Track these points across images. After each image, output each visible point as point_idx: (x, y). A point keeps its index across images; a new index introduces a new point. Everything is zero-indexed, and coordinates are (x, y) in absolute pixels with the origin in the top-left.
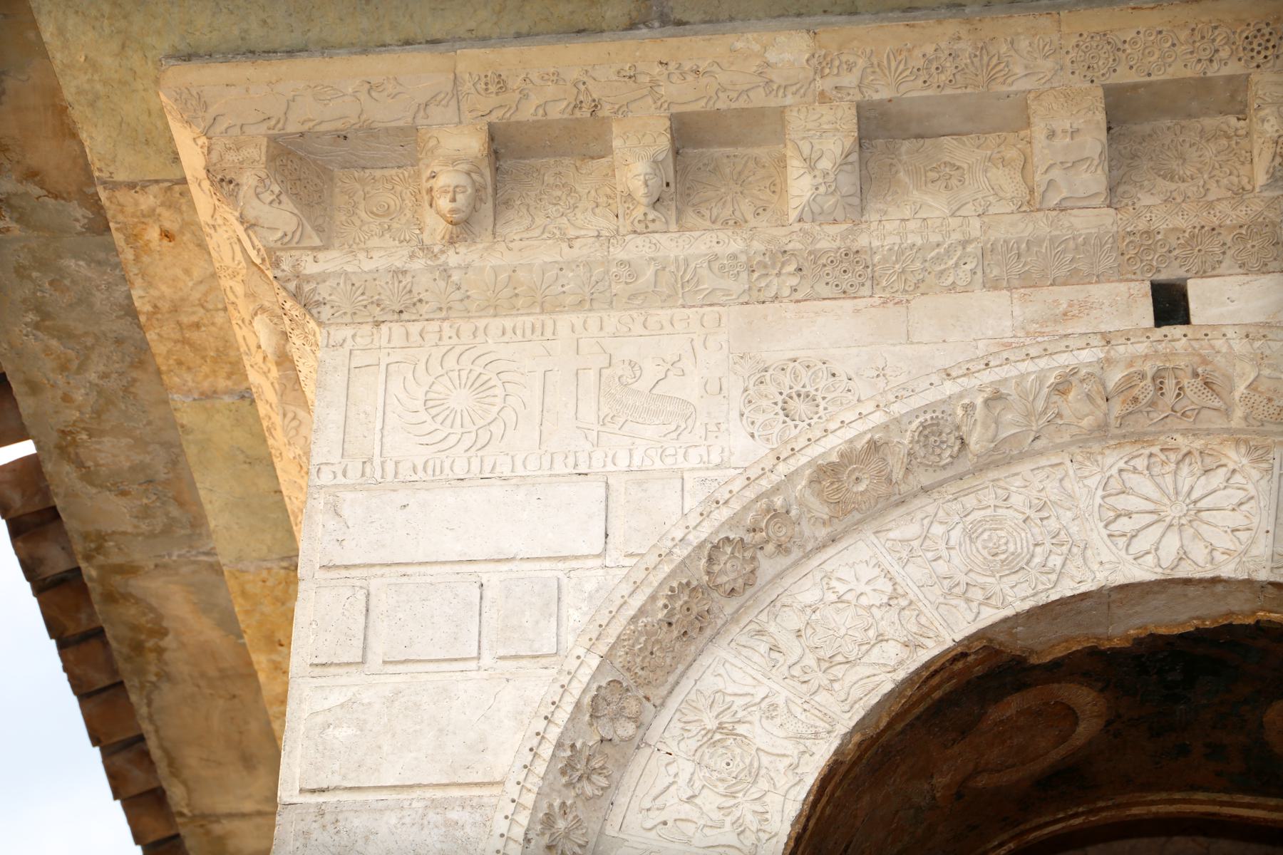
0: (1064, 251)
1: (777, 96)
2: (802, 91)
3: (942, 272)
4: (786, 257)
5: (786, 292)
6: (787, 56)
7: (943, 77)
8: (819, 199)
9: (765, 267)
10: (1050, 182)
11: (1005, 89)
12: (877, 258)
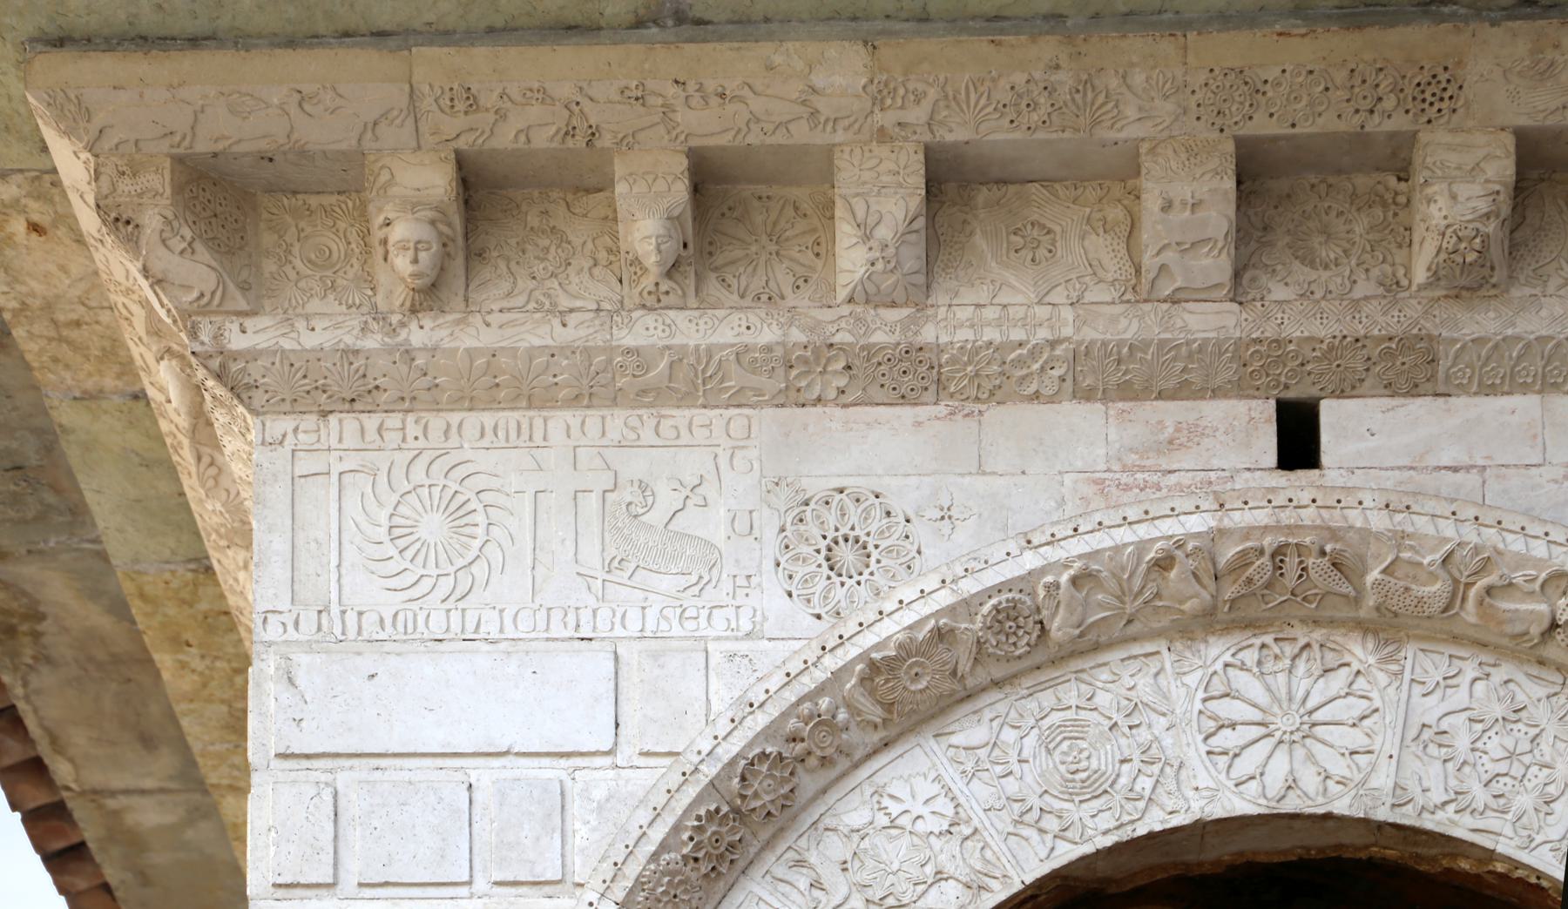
2: (856, 126)
7: (1035, 117)
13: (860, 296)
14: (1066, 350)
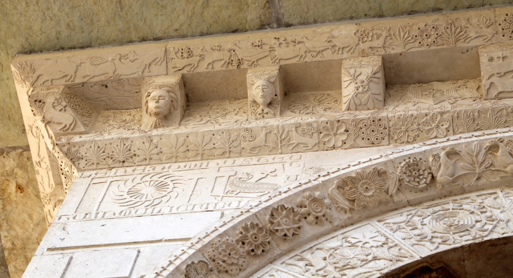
0: (501, 116)
1: (338, 53)
2: (352, 50)
3: (429, 131)
4: (340, 124)
5: (340, 144)
6: (344, 32)
7: (430, 40)
8: (359, 95)
9: (328, 130)
10: (491, 83)
11: (465, 45)
12: (391, 124)
13: (352, 106)
14: (448, 116)
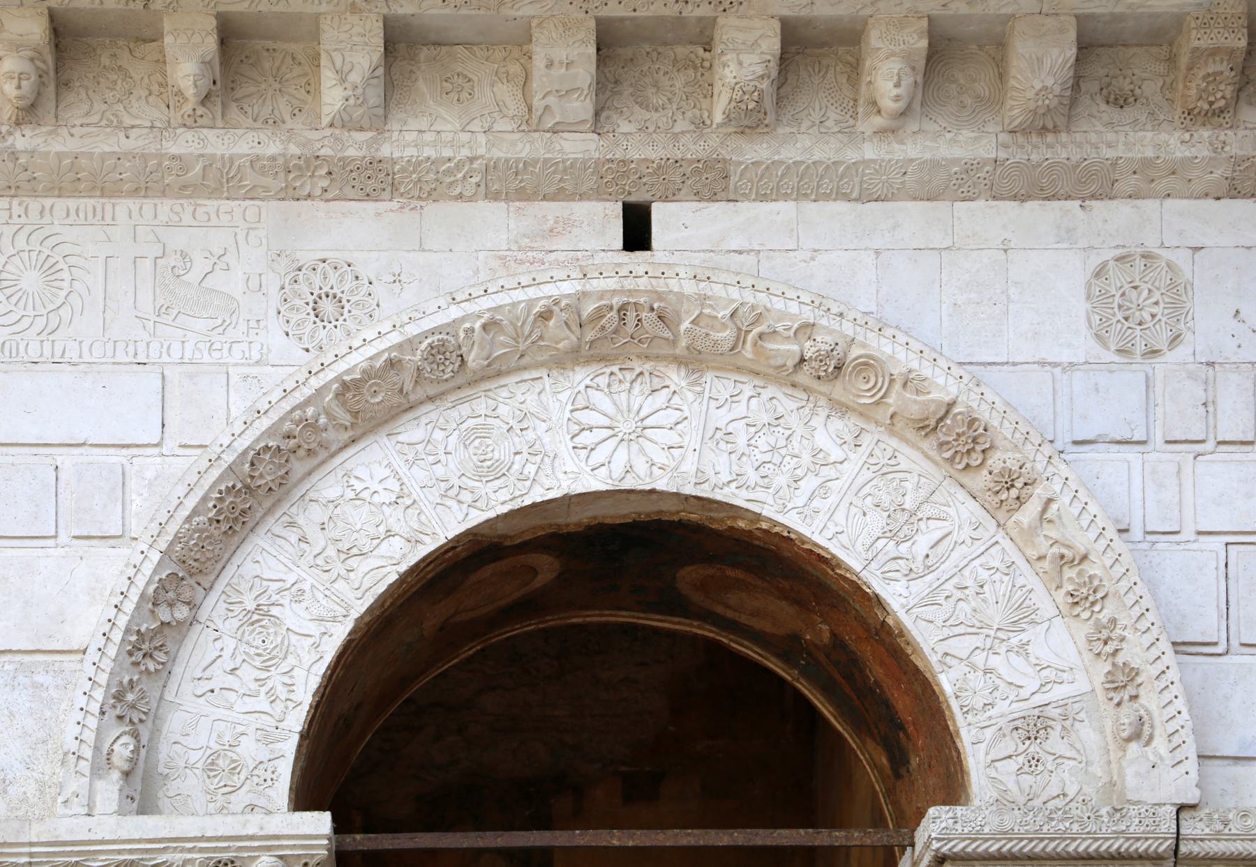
5: (318, 192)
10: (547, 107)
13: (338, 122)
